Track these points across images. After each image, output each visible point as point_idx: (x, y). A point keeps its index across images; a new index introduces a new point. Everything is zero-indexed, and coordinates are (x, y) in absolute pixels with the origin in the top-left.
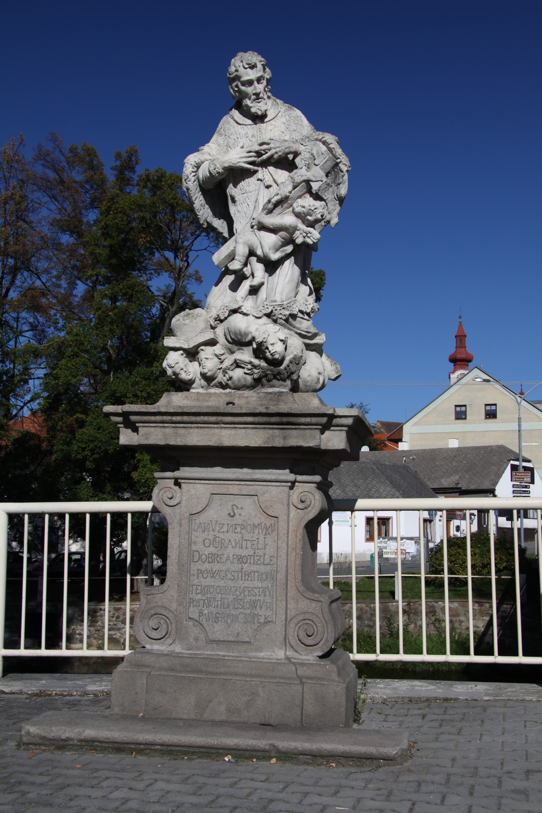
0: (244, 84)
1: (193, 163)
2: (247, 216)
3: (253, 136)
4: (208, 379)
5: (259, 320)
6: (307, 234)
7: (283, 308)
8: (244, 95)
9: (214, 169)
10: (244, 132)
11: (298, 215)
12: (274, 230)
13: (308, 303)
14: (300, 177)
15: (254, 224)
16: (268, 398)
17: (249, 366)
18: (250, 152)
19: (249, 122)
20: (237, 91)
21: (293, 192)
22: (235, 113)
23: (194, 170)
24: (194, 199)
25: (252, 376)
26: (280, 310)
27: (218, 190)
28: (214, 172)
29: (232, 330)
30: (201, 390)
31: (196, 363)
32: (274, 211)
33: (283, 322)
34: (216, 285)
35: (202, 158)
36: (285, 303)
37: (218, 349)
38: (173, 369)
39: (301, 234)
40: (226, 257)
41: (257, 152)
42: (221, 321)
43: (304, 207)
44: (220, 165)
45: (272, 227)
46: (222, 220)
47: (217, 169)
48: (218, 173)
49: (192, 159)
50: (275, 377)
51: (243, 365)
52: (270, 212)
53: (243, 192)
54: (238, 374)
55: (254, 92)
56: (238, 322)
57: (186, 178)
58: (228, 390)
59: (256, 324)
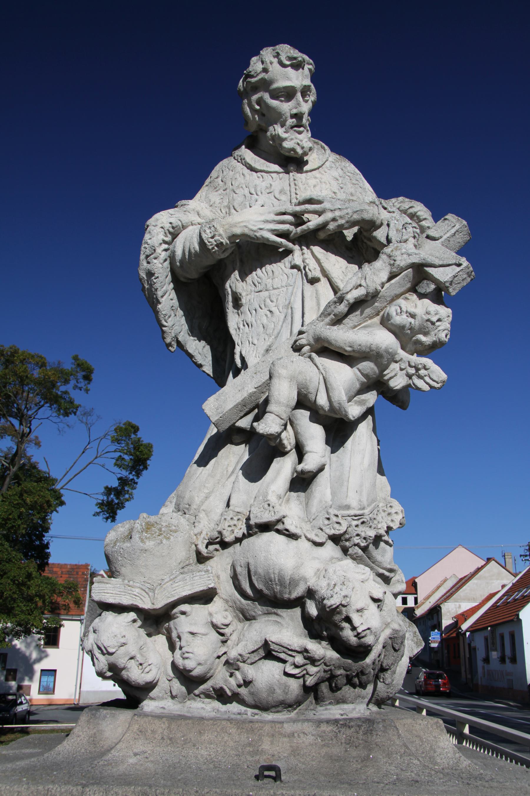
0: (276, 95)
1: (167, 226)
2: (270, 331)
3: (281, 192)
4: (190, 681)
5: (320, 550)
6: (417, 370)
7: (363, 523)
8: (270, 116)
9: (212, 237)
10: (264, 184)
11: (398, 332)
12: (347, 357)
13: (393, 511)
14: (405, 256)
15: (303, 341)
16: (343, 737)
17: (299, 659)
18: (284, 214)
19: (276, 168)
20: (256, 111)
21: (387, 285)
22: (245, 153)
23: (167, 239)
24: (159, 293)
25: (301, 680)
26: (357, 526)
27: (207, 285)
28: (211, 243)
29: (260, 571)
30: (171, 706)
31: (161, 640)
32: (346, 321)
33: (360, 552)
34: (203, 462)
35: (186, 218)
36: (366, 511)
37: (218, 611)
38: (112, 659)
39: (401, 369)
40: (236, 406)
41: (295, 215)
42: (224, 545)
43: (413, 316)
44: (225, 231)
45: (349, 349)
46: (203, 343)
47: (217, 238)
48: (220, 245)
49: (161, 221)
50: (349, 681)
51: (282, 656)
52: (338, 321)
53: (259, 288)
54: (267, 675)
55: (294, 111)
56: (274, 554)
57: (148, 252)
58: (234, 707)
59: (314, 558)
